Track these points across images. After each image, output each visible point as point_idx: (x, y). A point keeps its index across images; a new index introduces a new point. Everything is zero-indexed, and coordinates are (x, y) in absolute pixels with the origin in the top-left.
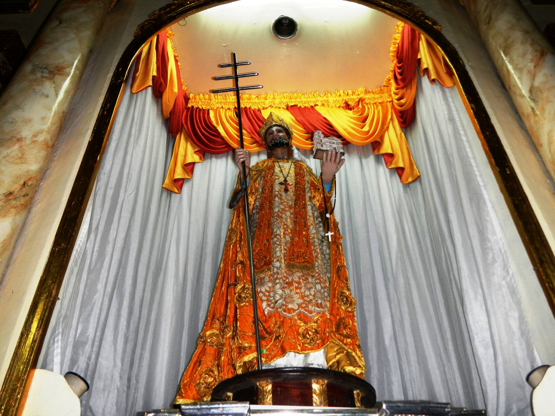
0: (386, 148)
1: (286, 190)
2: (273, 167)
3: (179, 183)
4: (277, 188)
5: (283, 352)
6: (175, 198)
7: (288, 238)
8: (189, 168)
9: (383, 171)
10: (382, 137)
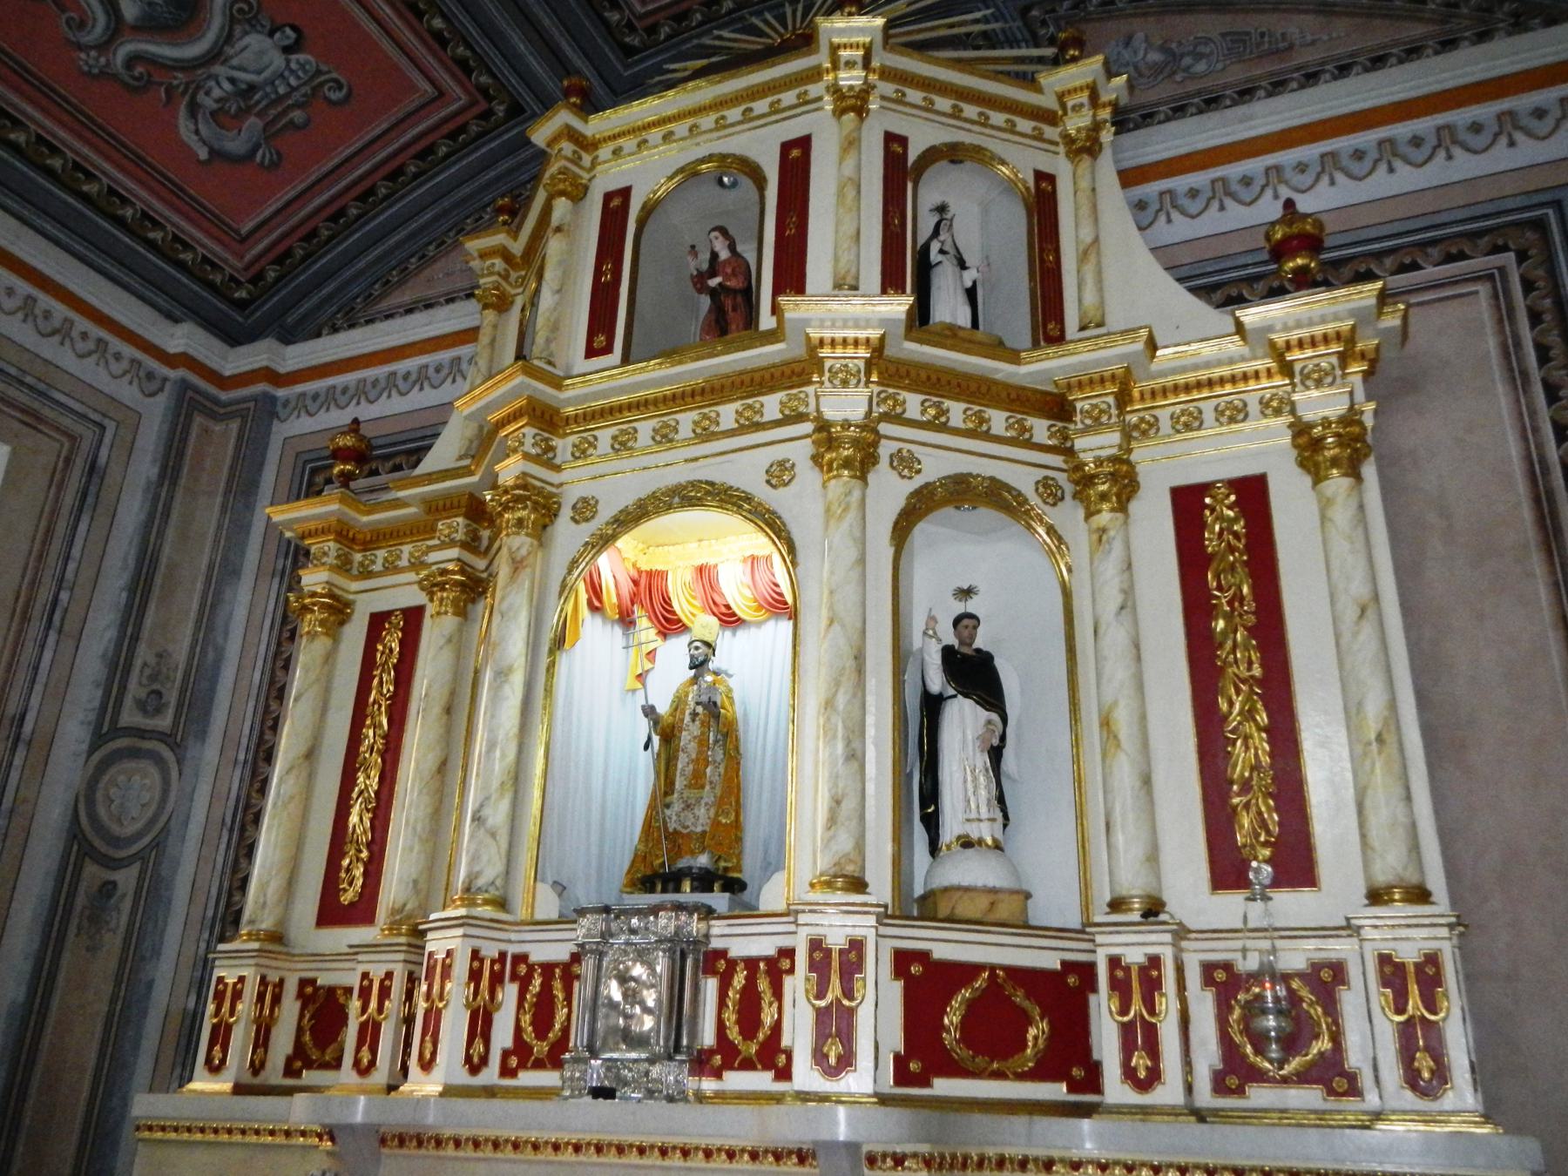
1: (693, 721)
7: (691, 767)
8: (651, 655)
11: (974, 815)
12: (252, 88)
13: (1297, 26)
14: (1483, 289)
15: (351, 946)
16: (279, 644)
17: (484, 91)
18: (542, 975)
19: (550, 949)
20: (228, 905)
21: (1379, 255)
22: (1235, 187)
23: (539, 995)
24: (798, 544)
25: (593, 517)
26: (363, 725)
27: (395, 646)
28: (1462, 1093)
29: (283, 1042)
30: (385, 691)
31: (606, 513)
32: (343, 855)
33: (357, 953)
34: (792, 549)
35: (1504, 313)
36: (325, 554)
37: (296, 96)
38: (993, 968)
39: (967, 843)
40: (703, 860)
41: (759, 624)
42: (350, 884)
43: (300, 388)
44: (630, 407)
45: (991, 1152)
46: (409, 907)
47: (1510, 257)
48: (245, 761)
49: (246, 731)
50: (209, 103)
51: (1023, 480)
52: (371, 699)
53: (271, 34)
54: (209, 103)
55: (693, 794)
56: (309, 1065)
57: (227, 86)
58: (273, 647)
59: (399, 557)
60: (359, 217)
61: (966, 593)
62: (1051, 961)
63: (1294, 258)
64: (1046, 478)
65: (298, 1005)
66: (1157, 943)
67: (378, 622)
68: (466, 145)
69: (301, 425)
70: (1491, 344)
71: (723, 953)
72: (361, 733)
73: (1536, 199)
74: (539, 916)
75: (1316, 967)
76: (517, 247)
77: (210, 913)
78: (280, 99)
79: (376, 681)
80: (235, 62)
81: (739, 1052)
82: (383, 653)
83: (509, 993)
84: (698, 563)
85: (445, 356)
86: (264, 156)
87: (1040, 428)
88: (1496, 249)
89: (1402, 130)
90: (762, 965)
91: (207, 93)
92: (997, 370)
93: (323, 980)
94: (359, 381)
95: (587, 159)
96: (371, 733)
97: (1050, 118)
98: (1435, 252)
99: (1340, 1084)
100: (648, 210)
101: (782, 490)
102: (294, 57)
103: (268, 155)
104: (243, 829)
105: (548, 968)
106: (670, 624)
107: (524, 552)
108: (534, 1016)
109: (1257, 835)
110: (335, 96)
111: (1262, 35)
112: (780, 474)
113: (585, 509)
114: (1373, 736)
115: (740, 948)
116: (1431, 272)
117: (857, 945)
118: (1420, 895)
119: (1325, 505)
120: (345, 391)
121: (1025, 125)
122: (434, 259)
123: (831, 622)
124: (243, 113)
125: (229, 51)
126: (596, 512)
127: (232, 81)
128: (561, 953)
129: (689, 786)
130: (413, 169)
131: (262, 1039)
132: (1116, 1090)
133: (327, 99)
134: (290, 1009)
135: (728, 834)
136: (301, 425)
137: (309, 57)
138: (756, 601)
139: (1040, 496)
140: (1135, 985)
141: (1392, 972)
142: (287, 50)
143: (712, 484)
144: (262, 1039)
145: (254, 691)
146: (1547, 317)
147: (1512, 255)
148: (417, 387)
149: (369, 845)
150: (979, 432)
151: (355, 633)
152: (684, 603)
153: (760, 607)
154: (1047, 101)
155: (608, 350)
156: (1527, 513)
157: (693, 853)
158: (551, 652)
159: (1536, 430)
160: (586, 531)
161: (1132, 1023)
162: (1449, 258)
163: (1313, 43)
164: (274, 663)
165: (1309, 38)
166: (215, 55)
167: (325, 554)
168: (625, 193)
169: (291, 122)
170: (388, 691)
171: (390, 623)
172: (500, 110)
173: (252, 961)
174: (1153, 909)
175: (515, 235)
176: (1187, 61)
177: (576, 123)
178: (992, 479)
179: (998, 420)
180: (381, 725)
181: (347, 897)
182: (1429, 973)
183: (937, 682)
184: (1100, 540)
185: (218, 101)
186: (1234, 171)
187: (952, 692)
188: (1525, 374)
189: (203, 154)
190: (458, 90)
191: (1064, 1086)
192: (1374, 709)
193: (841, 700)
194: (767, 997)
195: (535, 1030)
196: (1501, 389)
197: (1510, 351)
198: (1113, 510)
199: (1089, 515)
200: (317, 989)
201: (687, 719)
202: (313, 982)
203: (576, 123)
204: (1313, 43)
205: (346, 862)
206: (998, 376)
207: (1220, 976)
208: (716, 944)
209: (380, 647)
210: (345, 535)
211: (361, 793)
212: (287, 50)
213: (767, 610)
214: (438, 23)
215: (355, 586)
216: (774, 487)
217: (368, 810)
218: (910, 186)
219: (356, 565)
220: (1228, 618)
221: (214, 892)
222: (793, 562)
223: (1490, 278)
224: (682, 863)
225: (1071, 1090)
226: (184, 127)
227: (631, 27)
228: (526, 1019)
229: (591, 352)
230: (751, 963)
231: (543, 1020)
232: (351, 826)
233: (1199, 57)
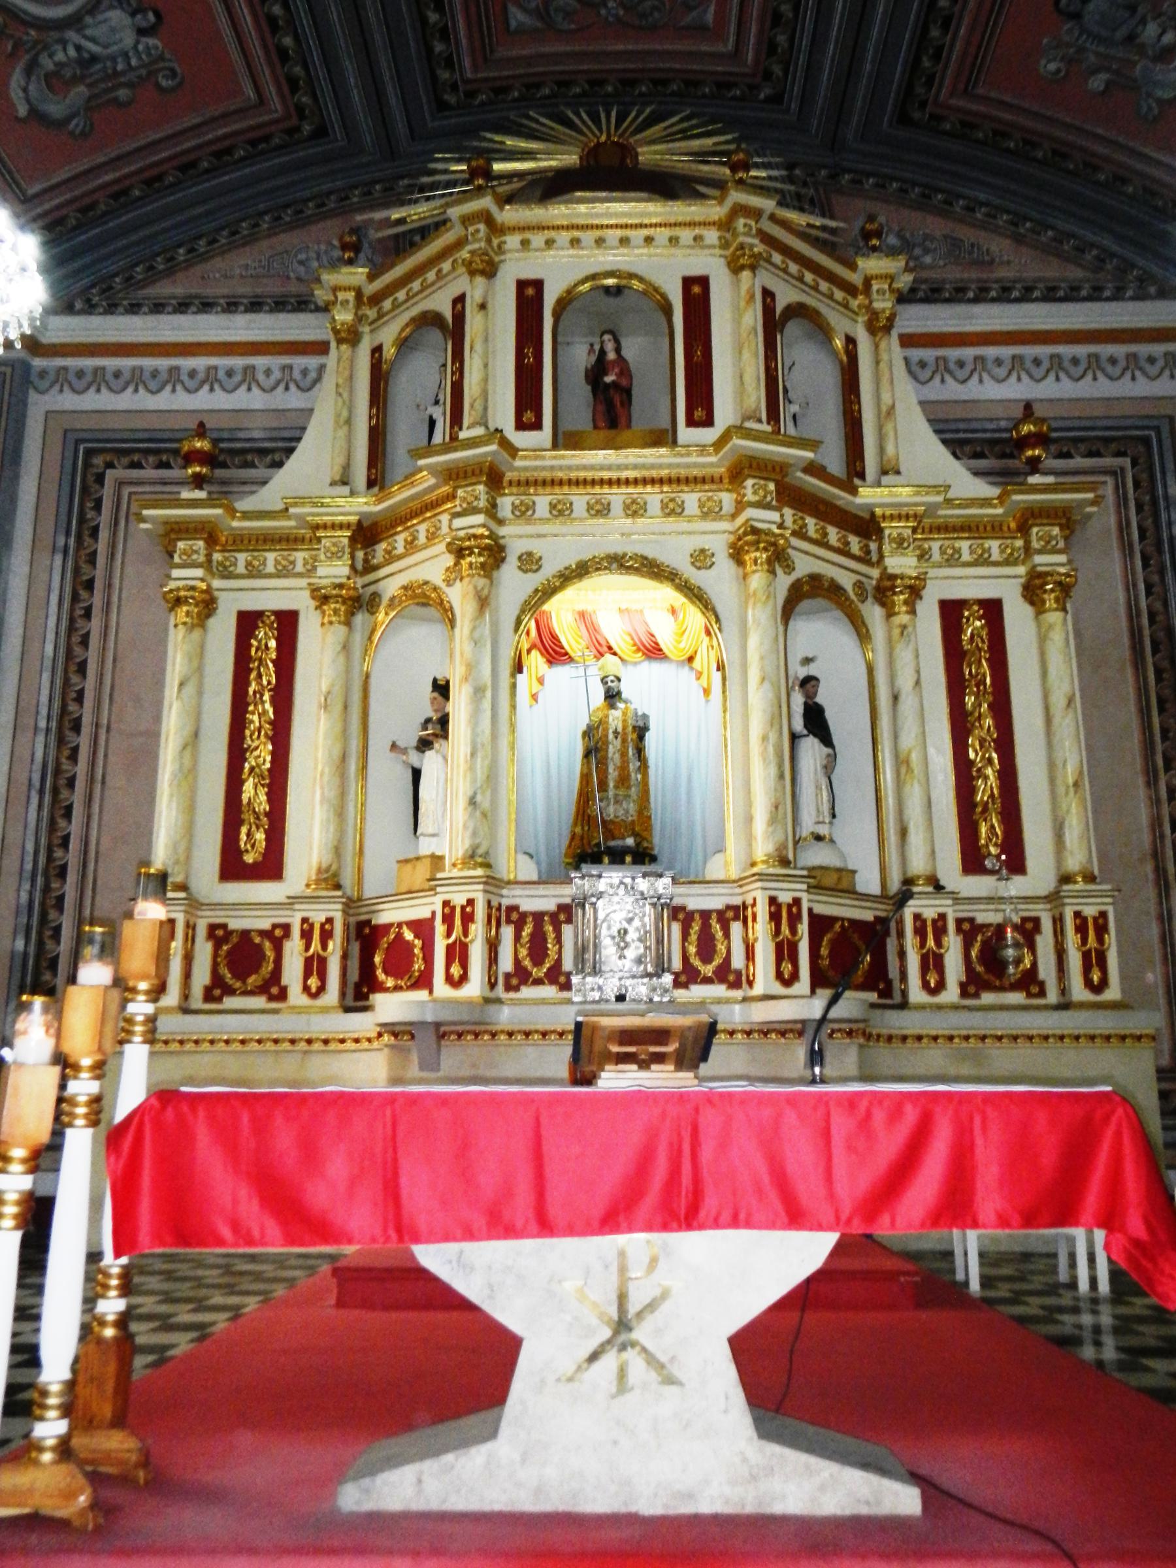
0: (697, 664)
2: (607, 716)
3: (535, 697)
4: (611, 736)
5: (614, 838)
6: (536, 707)
7: (616, 773)
8: (541, 681)
9: (695, 683)
10: (696, 652)
11: (821, 819)
12: (94, 59)
13: (999, 246)
14: (1110, 480)
15: (289, 897)
16: (72, 620)
17: (300, 110)
18: (534, 919)
19: (542, 900)
20: (50, 859)
22: (952, 366)
23: (533, 936)
24: (721, 617)
25: (537, 571)
26: (246, 712)
27: (273, 644)
29: (202, 976)
30: (265, 682)
31: (550, 569)
32: (241, 822)
33: (292, 904)
34: (718, 620)
35: (1121, 501)
36: (196, 552)
37: (131, 76)
38: (843, 919)
39: (819, 838)
40: (630, 841)
41: (635, 664)
42: (253, 846)
43: (60, 362)
44: (570, 482)
45: (885, 1031)
46: (334, 867)
47: (1126, 462)
48: (48, 730)
49: (44, 699)
50: (47, 63)
51: (846, 581)
52: (251, 690)
53: (133, 14)
54: (47, 63)
55: (621, 792)
56: (231, 992)
57: (72, 52)
58: (64, 623)
59: (264, 564)
60: (140, 198)
61: (807, 661)
62: (868, 916)
63: (1033, 448)
64: (860, 581)
65: (209, 947)
66: (943, 905)
67: (248, 622)
68: (262, 153)
69: (68, 401)
71: (683, 908)
72: (245, 719)
73: (1146, 422)
74: (521, 878)
75: (1024, 920)
76: (370, 289)
77: (29, 866)
78: (116, 74)
79: (253, 675)
80: (88, 32)
81: (699, 972)
82: (258, 649)
83: (508, 932)
84: (580, 608)
85: (238, 362)
86: (77, 125)
87: (855, 544)
88: (1120, 454)
89: (1066, 350)
90: (714, 915)
91: (51, 56)
92: (840, 498)
93: (235, 924)
94: (134, 369)
95: (495, 242)
96: (255, 718)
97: (851, 290)
98: (1082, 447)
99: (1035, 989)
100: (562, 305)
101: (703, 571)
102: (144, 40)
103: (82, 124)
104: (55, 791)
105: (538, 917)
106: (556, 654)
107: (486, 592)
108: (530, 948)
109: (991, 840)
110: (164, 83)
111: (973, 245)
112: (702, 558)
113: (529, 562)
114: (1071, 781)
115: (693, 904)
117: (797, 902)
120: (117, 374)
121: (839, 295)
122: (204, 258)
123: (763, 679)
124: (75, 80)
125: (88, 20)
126: (540, 567)
127: (78, 48)
128: (550, 905)
129: (616, 787)
130: (206, 164)
131: (187, 975)
132: (916, 995)
133: (157, 85)
134: (204, 951)
135: (642, 824)
136: (68, 401)
137: (159, 44)
138: (635, 644)
139: (856, 594)
140: (930, 930)
142: (141, 32)
143: (646, 558)
144: (187, 975)
145: (48, 663)
146: (1146, 508)
147: (1128, 460)
148: (206, 387)
149: (267, 814)
150: (822, 543)
151: (223, 629)
152: (571, 638)
153: (639, 650)
154: (856, 278)
155: (537, 425)
156: (1126, 640)
157: (623, 838)
158: (513, 675)
159: (1135, 585)
160: (534, 581)
161: (927, 953)
162: (1090, 454)
163: (1009, 263)
164: (69, 636)
165: (1005, 258)
166: (74, 21)
167: (196, 552)
168: (538, 284)
169: (116, 99)
170: (269, 683)
171: (263, 622)
172: (307, 128)
173: (182, 908)
174: (939, 888)
175: (372, 277)
176: (917, 251)
177: (494, 209)
178: (832, 580)
179: (833, 535)
180: (265, 712)
181: (249, 858)
183: (799, 725)
184: (902, 634)
185: (56, 64)
186: (953, 353)
187: (805, 732)
188: (1131, 545)
189: (22, 111)
190: (279, 107)
191: (876, 995)
193: (773, 737)
194: (719, 934)
195: (532, 959)
196: (1116, 554)
197: (1123, 527)
198: (908, 612)
199: (890, 614)
200: (229, 933)
201: (611, 736)
202: (224, 926)
203: (494, 209)
205: (244, 830)
206: (839, 503)
207: (966, 926)
208: (677, 901)
209: (254, 642)
210: (210, 534)
211: (252, 769)
212: (141, 32)
213: (644, 654)
214: (288, 41)
215: (217, 583)
216: (699, 568)
217: (263, 785)
218: (779, 337)
219: (215, 564)
220: (977, 695)
221: (30, 847)
222: (720, 629)
223: (1113, 473)
224: (612, 843)
225: (880, 996)
226: (17, 79)
227: (454, 87)
228: (523, 952)
229: (520, 426)
230: (705, 915)
231: (538, 950)
232: (245, 801)
233: (927, 251)
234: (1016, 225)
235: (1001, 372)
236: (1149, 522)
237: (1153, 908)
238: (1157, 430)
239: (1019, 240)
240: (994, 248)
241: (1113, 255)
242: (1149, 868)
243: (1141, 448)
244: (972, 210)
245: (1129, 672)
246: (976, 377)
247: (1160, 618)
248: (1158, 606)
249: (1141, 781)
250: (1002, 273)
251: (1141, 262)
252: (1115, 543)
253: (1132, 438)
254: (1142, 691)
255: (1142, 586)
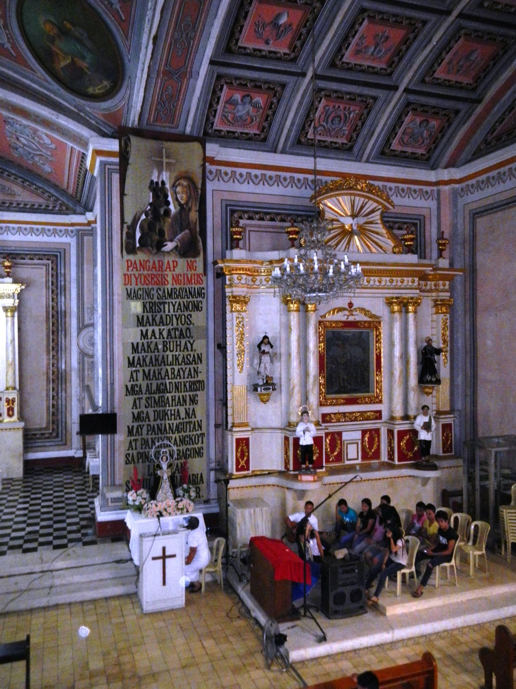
13: (17, 189)
14: (44, 267)
21: (27, 255)
28: (15, 418)
35: (47, 274)
47: (50, 262)
70: (44, 279)
88: (48, 259)
98: (37, 257)
116: (36, 261)
118: (14, 388)
119: (7, 322)
141: (8, 401)
156: (45, 314)
162: (40, 259)
182: (13, 401)
192: (10, 360)
197: (47, 281)
204: (20, 195)
223: (46, 265)
234: (23, 183)
235: (14, 232)
236: (55, 281)
237: (45, 388)
238: (60, 253)
239: (24, 187)
240: (16, 190)
241: (53, 195)
242: (45, 378)
243: (55, 258)
244: (10, 176)
245: (45, 324)
246: (6, 233)
247: (55, 308)
248: (55, 305)
249: (45, 353)
250: (19, 199)
251: (61, 198)
252: (44, 287)
253: (52, 255)
254: (48, 329)
255: (51, 299)
